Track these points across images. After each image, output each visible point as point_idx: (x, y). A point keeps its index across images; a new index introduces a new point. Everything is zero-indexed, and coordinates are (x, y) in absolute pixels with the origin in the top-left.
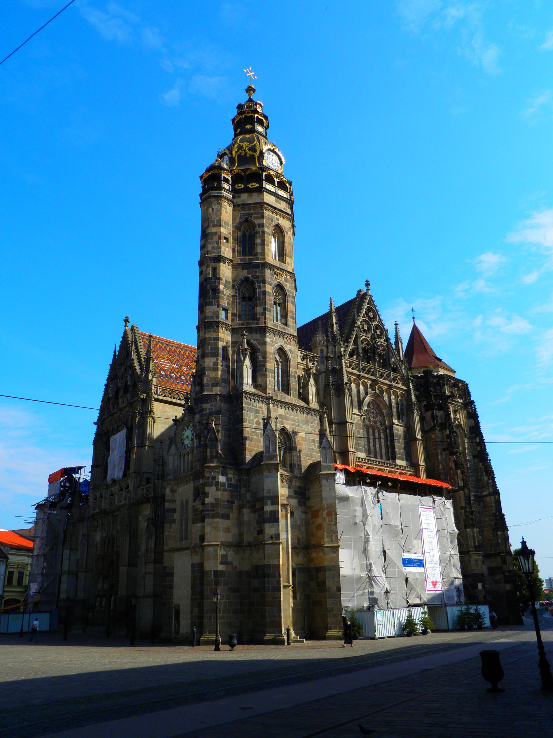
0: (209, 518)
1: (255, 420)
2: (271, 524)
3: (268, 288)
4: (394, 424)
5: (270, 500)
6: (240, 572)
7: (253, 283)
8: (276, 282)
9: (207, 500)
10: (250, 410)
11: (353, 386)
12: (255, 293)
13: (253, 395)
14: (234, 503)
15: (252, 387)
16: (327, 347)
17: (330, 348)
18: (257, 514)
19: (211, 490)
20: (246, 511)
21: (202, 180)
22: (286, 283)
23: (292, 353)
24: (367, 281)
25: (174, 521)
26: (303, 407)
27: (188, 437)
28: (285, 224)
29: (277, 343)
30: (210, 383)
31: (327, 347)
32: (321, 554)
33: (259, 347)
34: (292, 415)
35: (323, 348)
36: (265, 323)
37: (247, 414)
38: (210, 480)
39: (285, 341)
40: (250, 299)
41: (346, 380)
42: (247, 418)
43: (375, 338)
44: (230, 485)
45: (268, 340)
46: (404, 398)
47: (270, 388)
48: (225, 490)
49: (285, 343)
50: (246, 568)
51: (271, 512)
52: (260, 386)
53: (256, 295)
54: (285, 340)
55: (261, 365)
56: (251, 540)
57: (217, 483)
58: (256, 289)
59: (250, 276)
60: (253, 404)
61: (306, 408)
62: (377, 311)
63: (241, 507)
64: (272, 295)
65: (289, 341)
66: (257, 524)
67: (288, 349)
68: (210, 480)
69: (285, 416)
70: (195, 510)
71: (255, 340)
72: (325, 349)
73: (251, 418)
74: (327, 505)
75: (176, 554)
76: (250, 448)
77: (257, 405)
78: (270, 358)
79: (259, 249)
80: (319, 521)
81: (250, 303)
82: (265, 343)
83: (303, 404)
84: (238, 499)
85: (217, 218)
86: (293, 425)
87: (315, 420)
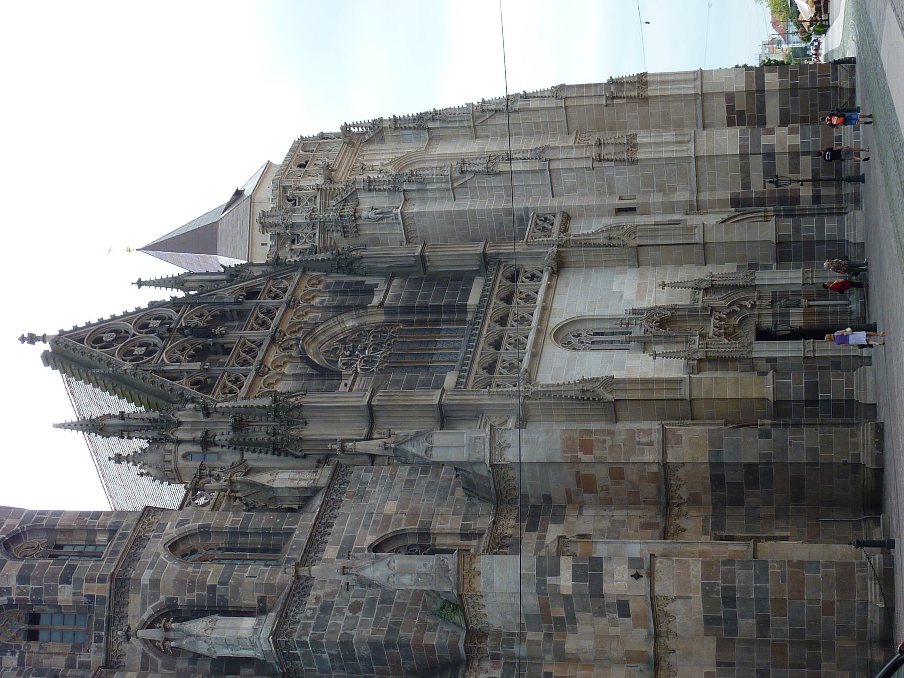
1: (348, 613)
2: (605, 578)
4: (381, 305)
5: (548, 578)
6: (719, 664)
11: (281, 387)
12: (22, 604)
14: (551, 673)
15: (264, 617)
16: (179, 442)
17: (180, 435)
18: (578, 615)
20: (571, 644)
22: (4, 526)
23: (187, 522)
24: (22, 339)
26: (325, 504)
29: (158, 555)
31: (179, 442)
32: (681, 472)
33: (162, 598)
34: (341, 527)
35: (180, 454)
37: (331, 632)
39: (154, 537)
40: (34, 618)
41: (267, 402)
42: (341, 631)
43: (169, 330)
46: (323, 278)
47: (269, 576)
49: (159, 537)
50: (707, 648)
51: (575, 577)
52: (262, 600)
53: (27, 600)
54: (152, 534)
55: (209, 596)
56: (642, 633)
58: (10, 600)
60: (307, 618)
63: (562, 657)
64: (32, 562)
65: (155, 527)
66: (605, 616)
67: (175, 530)
69: (343, 543)
71: (143, 609)
72: (183, 449)
73: (341, 622)
74: (564, 452)
76: (415, 629)
77: (310, 609)
78: (193, 572)
80: (602, 474)
81: (44, 620)
83: (318, 502)
84: (541, 664)
86: (366, 527)
87: (358, 476)
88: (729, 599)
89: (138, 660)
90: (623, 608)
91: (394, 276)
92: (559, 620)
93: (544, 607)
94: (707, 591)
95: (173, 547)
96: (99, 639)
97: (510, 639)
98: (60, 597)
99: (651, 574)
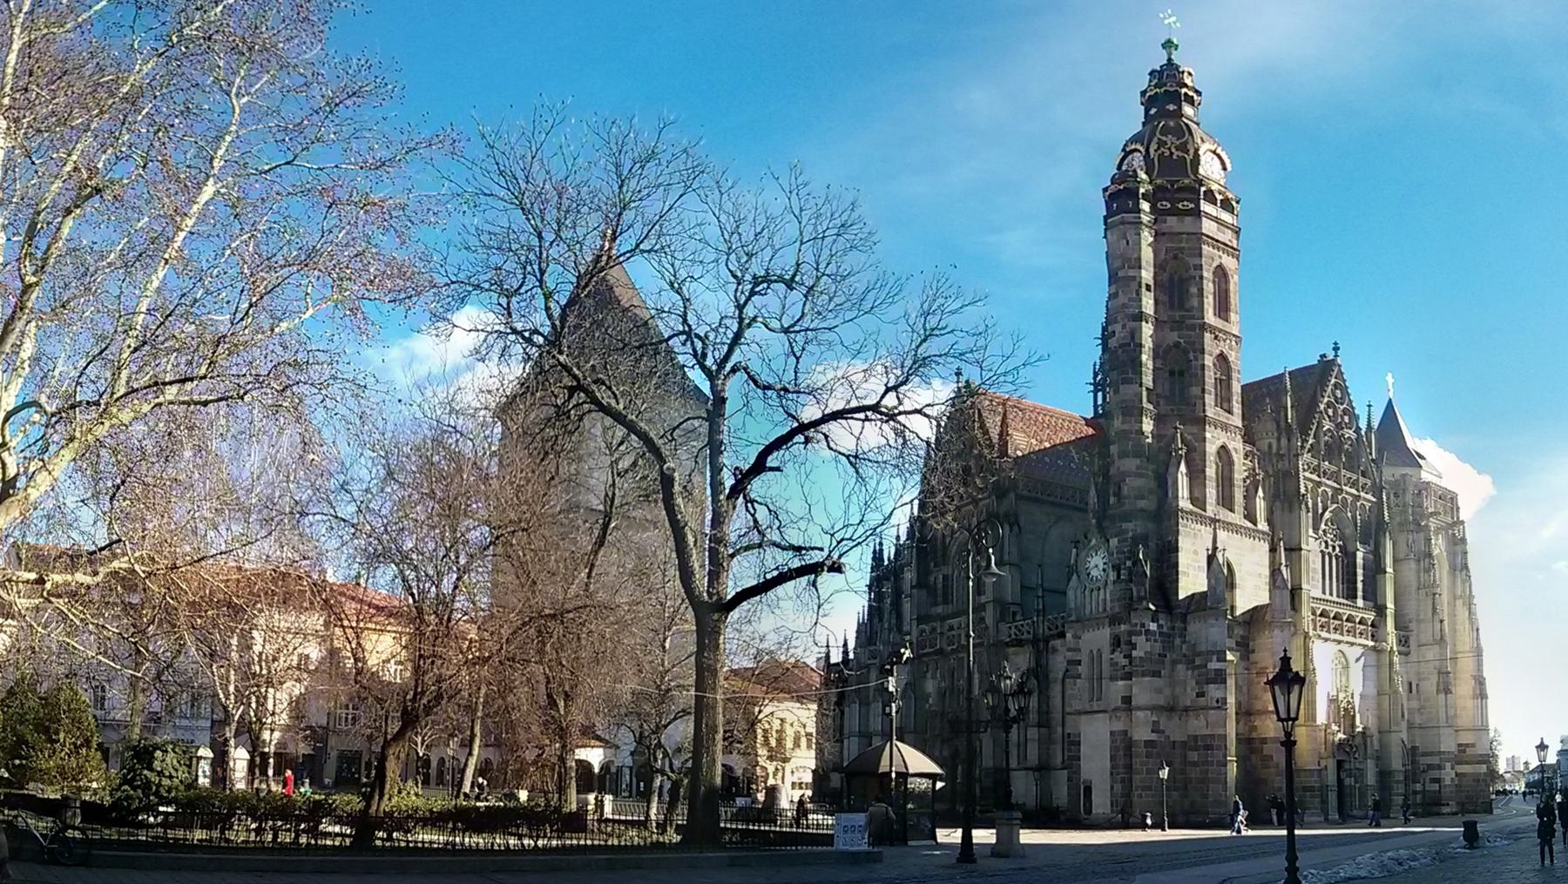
0: (1137, 676)
3: (1209, 361)
6: (1174, 742)
7: (1186, 352)
8: (1218, 352)
9: (1135, 653)
10: (1188, 534)
13: (1191, 513)
16: (1279, 440)
19: (1140, 640)
20: (1180, 667)
21: (1107, 194)
25: (1079, 677)
26: (1249, 529)
27: (1097, 566)
28: (1229, 262)
30: (1132, 494)
31: (1279, 440)
33: (1197, 444)
36: (1204, 411)
38: (1138, 628)
41: (1303, 490)
44: (1161, 634)
45: (1208, 435)
48: (1155, 641)
52: (1197, 499)
57: (1148, 632)
59: (1182, 341)
61: (1254, 531)
62: (1346, 387)
63: (1174, 663)
68: (1138, 628)
70: (1114, 664)
71: (1192, 434)
72: (1274, 443)
75: (1083, 717)
79: (1195, 302)
82: (1204, 439)
83: (1250, 525)
85: (1136, 256)
88: (1208, 747)
89: (1163, 432)
90: (1201, 694)
91: (1375, 556)
92: (1194, 662)
93: (1199, 654)
94: (1212, 736)
95: (1223, 447)
96: (1172, 410)
97: (1183, 636)
98: (1194, 388)
99: (1219, 708)
